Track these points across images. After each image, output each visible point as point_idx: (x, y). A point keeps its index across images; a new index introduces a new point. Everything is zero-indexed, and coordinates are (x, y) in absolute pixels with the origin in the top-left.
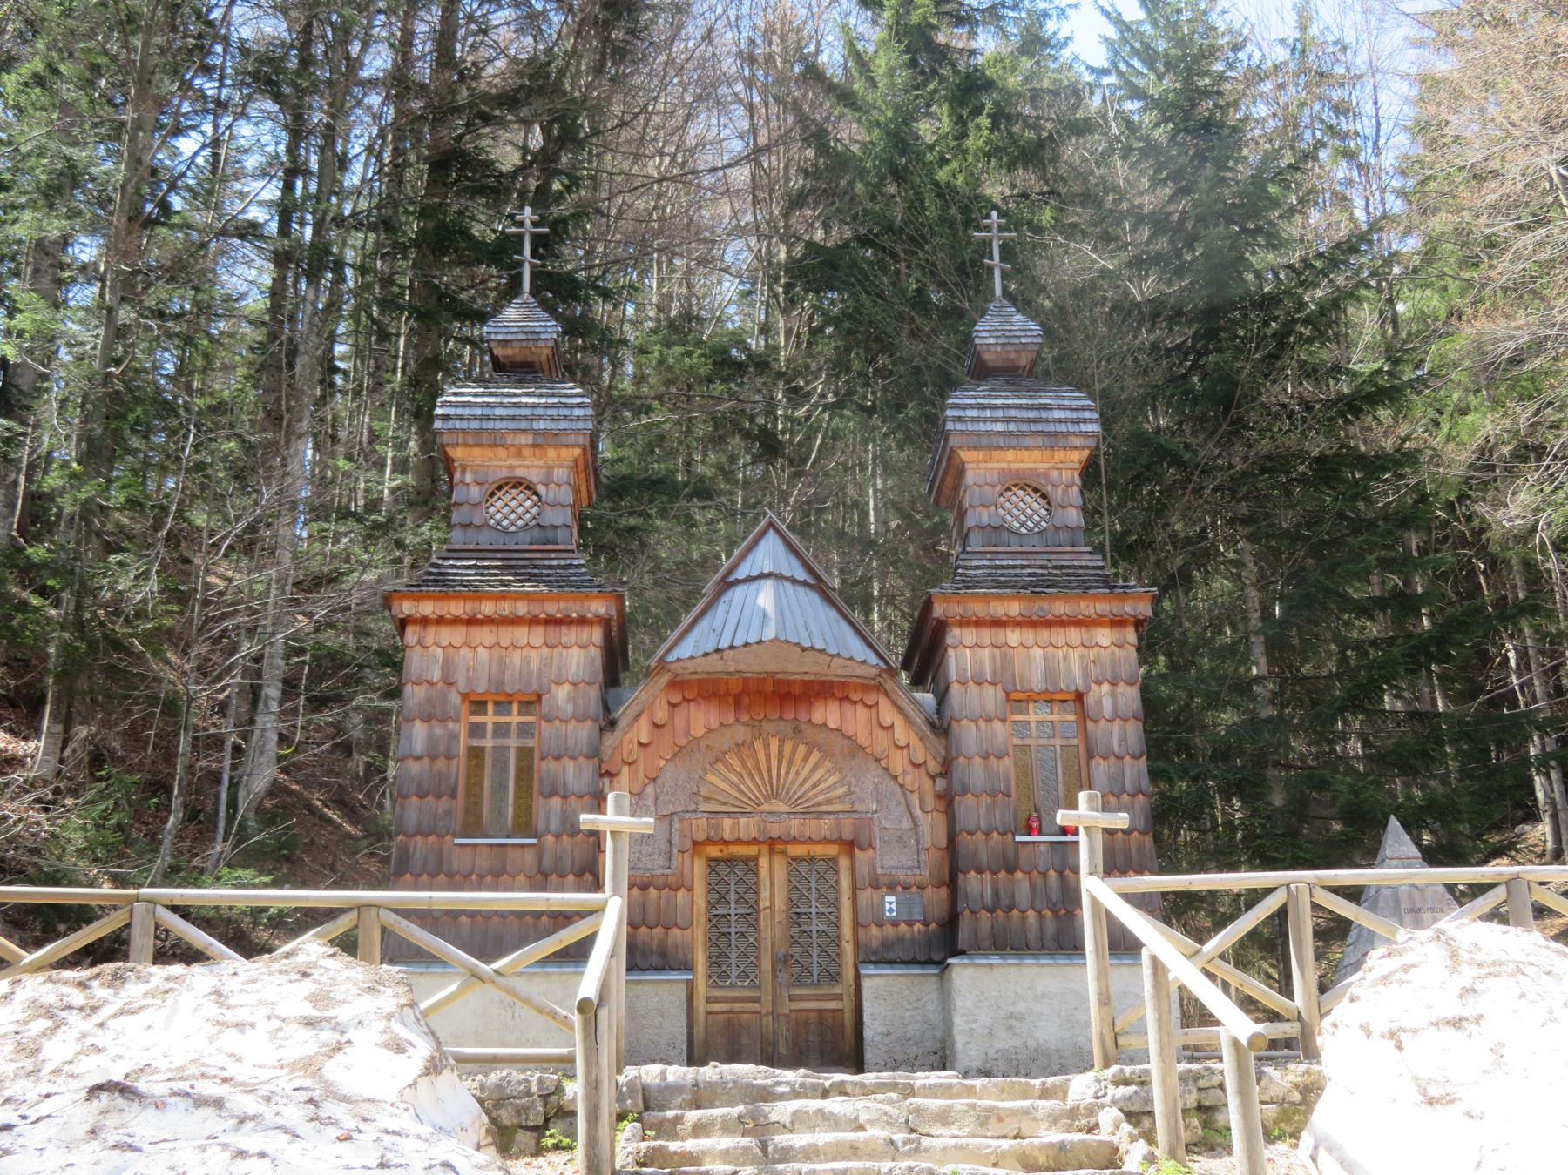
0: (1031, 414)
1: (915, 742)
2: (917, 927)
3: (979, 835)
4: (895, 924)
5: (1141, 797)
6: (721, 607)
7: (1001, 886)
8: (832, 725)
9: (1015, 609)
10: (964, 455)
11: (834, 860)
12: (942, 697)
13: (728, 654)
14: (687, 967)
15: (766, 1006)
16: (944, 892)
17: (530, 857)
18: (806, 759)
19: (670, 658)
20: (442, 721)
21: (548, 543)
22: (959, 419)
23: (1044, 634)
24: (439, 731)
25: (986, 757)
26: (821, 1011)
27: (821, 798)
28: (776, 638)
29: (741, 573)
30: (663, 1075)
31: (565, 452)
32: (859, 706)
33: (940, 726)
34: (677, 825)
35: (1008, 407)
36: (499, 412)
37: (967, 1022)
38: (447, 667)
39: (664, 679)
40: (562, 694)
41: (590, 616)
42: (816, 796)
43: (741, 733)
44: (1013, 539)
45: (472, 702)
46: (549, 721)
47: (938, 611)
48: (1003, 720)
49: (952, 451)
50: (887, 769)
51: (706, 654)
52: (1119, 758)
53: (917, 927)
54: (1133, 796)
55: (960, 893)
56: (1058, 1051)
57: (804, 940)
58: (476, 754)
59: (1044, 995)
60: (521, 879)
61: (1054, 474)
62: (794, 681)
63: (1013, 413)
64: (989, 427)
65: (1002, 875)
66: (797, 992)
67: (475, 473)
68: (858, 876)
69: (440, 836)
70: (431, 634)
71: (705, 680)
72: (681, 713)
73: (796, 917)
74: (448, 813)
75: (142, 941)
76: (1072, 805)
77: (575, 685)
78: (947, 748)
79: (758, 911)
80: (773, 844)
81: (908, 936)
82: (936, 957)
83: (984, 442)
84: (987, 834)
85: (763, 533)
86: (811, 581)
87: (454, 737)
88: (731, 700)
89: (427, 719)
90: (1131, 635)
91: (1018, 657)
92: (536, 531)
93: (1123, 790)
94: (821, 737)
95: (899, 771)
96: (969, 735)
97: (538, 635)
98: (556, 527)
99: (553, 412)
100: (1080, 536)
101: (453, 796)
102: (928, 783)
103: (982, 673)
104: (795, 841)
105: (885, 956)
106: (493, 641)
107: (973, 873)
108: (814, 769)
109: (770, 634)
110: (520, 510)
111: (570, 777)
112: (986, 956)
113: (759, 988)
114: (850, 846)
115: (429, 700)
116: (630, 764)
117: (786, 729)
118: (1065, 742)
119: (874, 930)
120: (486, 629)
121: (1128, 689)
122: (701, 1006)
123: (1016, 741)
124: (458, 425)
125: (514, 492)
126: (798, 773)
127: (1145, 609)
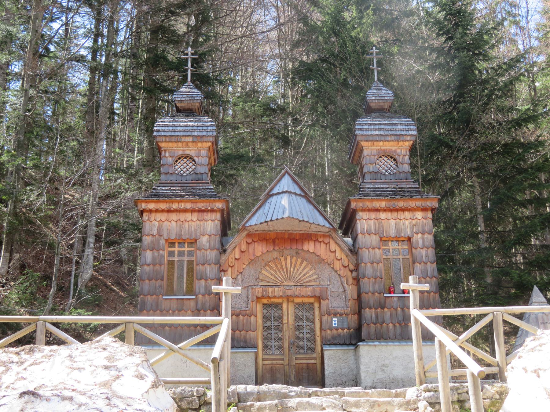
0: (390, 127)
1: (344, 257)
2: (346, 330)
3: (370, 294)
4: (337, 329)
5: (434, 278)
6: (267, 205)
7: (379, 314)
8: (311, 251)
9: (383, 204)
10: (363, 144)
11: (313, 304)
12: (355, 240)
13: (270, 223)
14: (255, 346)
15: (286, 362)
16: (356, 317)
17: (192, 304)
18: (301, 264)
19: (247, 225)
20: (158, 250)
21: (199, 180)
22: (361, 129)
23: (395, 214)
24: (156, 254)
25: (372, 263)
26: (308, 364)
27: (307, 280)
28: (289, 217)
29: (275, 191)
30: (246, 388)
31: (205, 144)
32: (322, 243)
33: (354, 251)
34: (250, 291)
35: (380, 125)
36: (179, 128)
37: (366, 368)
38: (160, 229)
39: (245, 233)
40: (204, 240)
41: (215, 208)
42: (305, 279)
43: (275, 254)
44: (383, 177)
45: (170, 243)
46: (200, 250)
47: (353, 205)
48: (379, 249)
49: (358, 142)
50: (333, 268)
51: (261, 223)
52: (426, 263)
53: (346, 330)
54: (431, 278)
55: (363, 317)
56: (402, 379)
57: (301, 336)
58: (171, 263)
59: (396, 357)
60: (189, 312)
61: (399, 151)
62: (296, 234)
63: (382, 127)
64: (373, 132)
65: (379, 310)
66: (298, 356)
67: (170, 153)
68: (322, 310)
69: (158, 296)
70: (153, 216)
71: (261, 233)
72: (251, 247)
73: (298, 327)
74: (160, 286)
75: (41, 336)
76: (407, 281)
77: (210, 236)
78: (357, 260)
79: (282, 324)
80: (289, 298)
81: (342, 334)
82: (353, 342)
83: (371, 138)
84: (373, 293)
85: (283, 175)
86: (302, 194)
87: (162, 256)
88: (271, 241)
89: (152, 250)
90: (430, 215)
91: (385, 223)
92: (194, 176)
93: (427, 276)
94: (307, 256)
95: (338, 269)
96: (366, 254)
97: (195, 216)
98: (202, 174)
99: (200, 128)
100: (409, 175)
101: (162, 280)
102: (349, 273)
103: (371, 230)
104: (297, 297)
105: (333, 342)
106: (178, 219)
107: (367, 309)
108: (304, 268)
109: (286, 215)
110: (188, 167)
111: (208, 272)
112: (373, 342)
113: (283, 355)
114: (319, 299)
115: (152, 242)
116: (232, 267)
117: (293, 252)
118: (404, 257)
119: (329, 332)
120: (174, 214)
121: (429, 236)
122: (260, 362)
123: (384, 257)
124: (163, 134)
125: (185, 160)
126: (298, 270)
127: (435, 204)
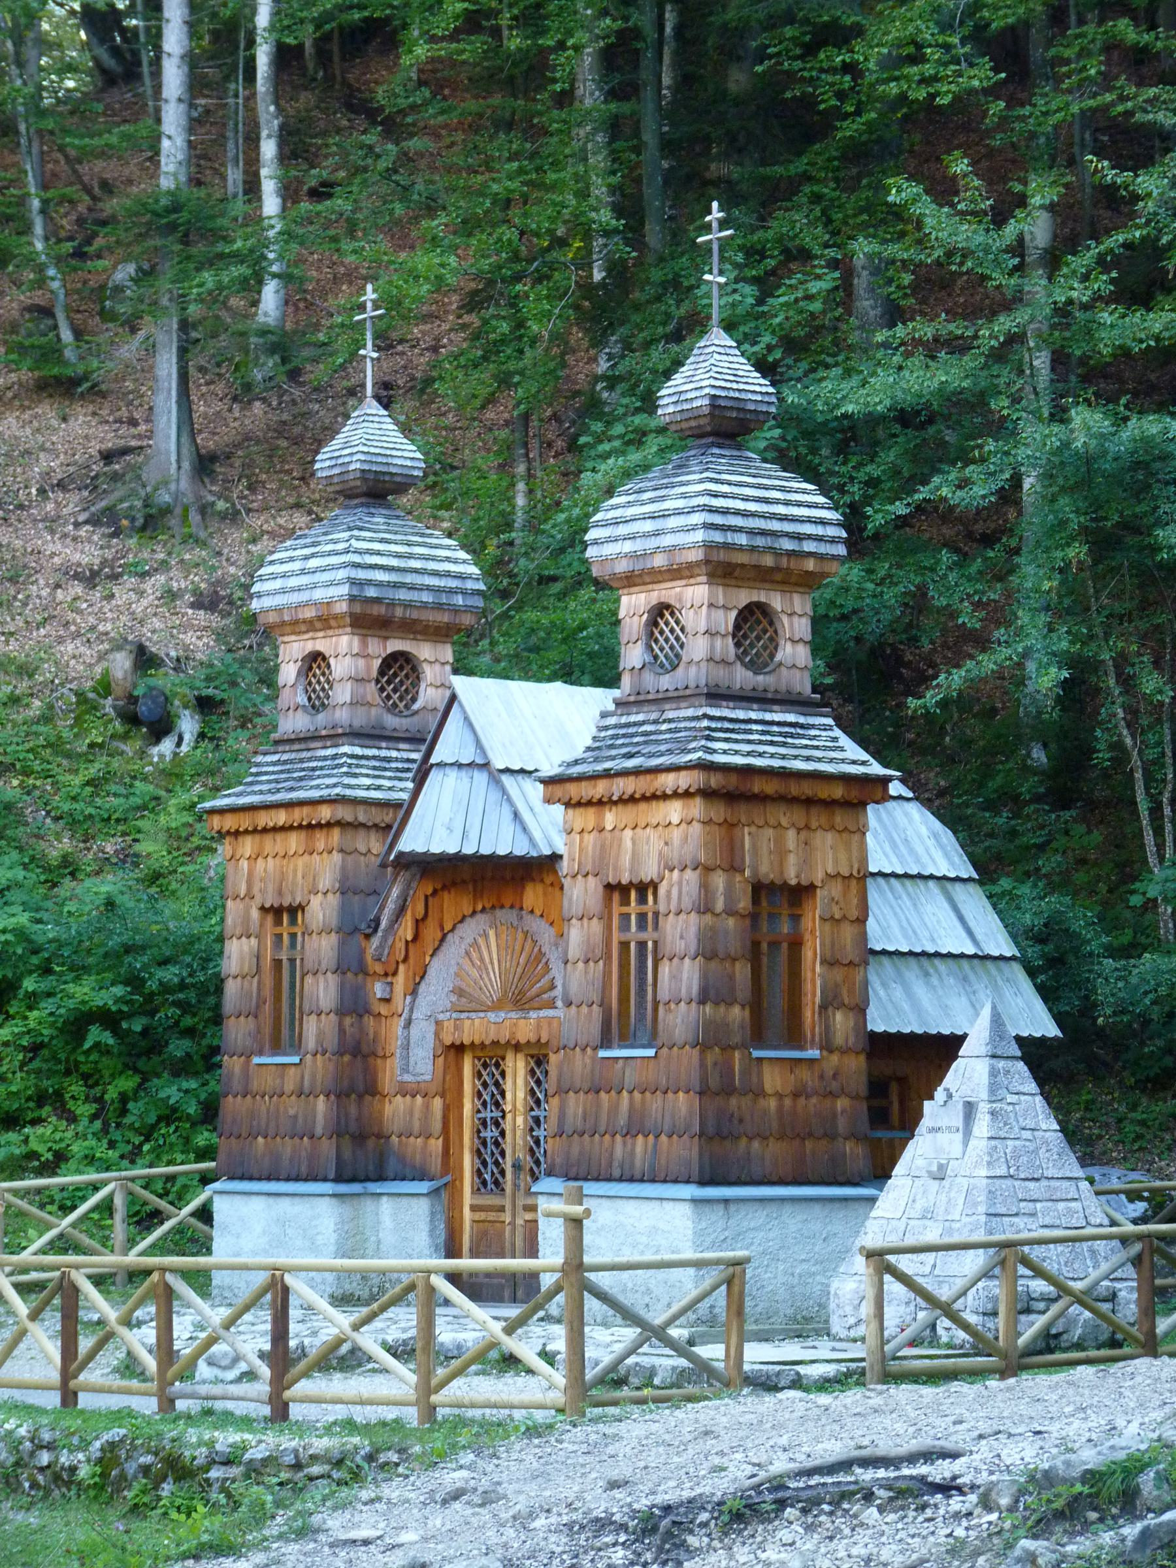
25: (587, 961)
